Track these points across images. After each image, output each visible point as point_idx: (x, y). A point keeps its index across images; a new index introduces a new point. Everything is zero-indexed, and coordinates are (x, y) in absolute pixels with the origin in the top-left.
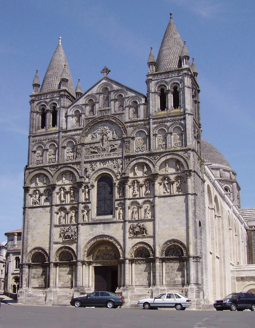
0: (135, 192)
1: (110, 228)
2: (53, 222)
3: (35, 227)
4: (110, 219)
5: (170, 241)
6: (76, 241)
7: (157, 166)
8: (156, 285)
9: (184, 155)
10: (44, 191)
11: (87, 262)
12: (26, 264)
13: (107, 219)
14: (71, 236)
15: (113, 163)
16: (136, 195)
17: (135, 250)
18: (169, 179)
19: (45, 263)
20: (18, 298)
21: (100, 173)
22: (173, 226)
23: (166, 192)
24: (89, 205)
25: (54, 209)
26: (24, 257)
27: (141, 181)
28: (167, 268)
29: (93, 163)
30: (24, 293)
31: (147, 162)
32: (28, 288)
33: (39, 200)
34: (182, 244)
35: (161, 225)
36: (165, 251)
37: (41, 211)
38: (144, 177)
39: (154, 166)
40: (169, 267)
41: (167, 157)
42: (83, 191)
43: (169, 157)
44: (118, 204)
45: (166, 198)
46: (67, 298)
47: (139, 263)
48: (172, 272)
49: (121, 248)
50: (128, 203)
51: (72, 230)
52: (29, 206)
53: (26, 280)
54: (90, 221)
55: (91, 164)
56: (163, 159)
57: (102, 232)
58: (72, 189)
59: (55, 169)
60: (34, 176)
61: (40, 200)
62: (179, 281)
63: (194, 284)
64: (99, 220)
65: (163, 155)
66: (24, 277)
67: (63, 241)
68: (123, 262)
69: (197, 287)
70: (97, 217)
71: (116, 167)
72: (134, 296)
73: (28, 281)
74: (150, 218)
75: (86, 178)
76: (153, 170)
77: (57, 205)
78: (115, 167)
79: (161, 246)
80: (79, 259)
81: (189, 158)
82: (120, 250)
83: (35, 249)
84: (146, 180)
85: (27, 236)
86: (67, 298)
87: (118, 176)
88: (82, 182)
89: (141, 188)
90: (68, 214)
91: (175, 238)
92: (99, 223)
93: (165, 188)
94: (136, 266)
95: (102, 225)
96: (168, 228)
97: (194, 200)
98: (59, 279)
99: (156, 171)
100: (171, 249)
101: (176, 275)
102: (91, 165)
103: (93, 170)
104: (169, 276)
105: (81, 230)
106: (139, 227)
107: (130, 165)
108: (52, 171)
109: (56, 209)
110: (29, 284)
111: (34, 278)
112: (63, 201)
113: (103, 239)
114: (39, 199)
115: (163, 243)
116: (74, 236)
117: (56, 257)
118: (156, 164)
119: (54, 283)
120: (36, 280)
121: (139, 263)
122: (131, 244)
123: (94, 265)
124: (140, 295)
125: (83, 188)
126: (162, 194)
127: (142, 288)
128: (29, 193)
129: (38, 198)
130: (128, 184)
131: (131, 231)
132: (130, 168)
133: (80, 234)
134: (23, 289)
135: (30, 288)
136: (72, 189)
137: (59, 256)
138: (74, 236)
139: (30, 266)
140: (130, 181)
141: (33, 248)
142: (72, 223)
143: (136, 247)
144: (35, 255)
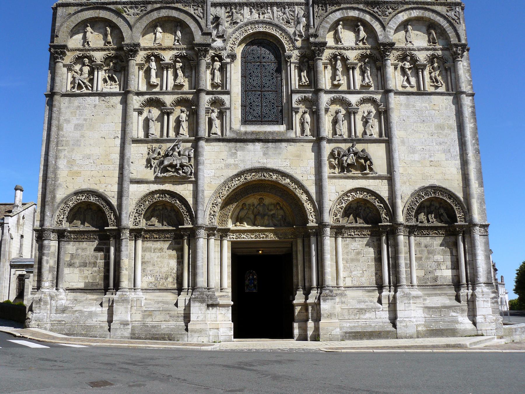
0: (337, 78)
1: (280, 154)
2: (128, 130)
3: (78, 141)
4: (278, 133)
5: (424, 189)
6: (194, 179)
7: (390, 28)
8: (400, 286)
9: (448, 14)
10: (106, 59)
11: (220, 230)
12: (54, 231)
13: (272, 133)
14: (178, 165)
15: (284, 13)
16: (339, 85)
17: (344, 205)
18: (414, 60)
19: (106, 228)
20: (30, 315)
21: (252, 32)
22: (431, 156)
23: (407, 85)
24: (225, 97)
25: (132, 101)
26: (48, 213)
27: (352, 56)
28: (418, 249)
29: (233, 7)
30: (46, 303)
31: (368, 18)
32: (56, 289)
33: (91, 81)
34: (451, 195)
35: (403, 155)
36: (414, 211)
37: (95, 106)
38: (359, 49)
39: (384, 27)
40: (420, 247)
41: (411, 14)
42: (208, 68)
43: (415, 13)
44: (300, 102)
45: (412, 98)
46: (168, 317)
47: (350, 235)
48: (428, 258)
49: (310, 198)
50: (325, 99)
51: (182, 153)
52: (64, 91)
53: (51, 269)
54: (229, 134)
55: (228, 10)
56: (403, 16)
57: (261, 161)
58: (178, 59)
59: (139, 12)
60: (80, 22)
61: (93, 79)
62: (445, 278)
63: (484, 283)
64: (252, 133)
65: (403, 8)
66: (47, 263)
67: (156, 177)
68: (319, 232)
69: (491, 291)
70: (244, 127)
71: (291, 21)
72: (346, 310)
73: (55, 273)
74: (376, 136)
75: (216, 39)
76: (381, 35)
77: (139, 94)
78: (288, 22)
79: (406, 199)
80: (200, 221)
81: (458, 21)
82: (308, 206)
83: (76, 193)
84: (362, 58)
85: (55, 163)
86: (168, 315)
87: (297, 40)
88: (209, 45)
89: (351, 71)
90: (168, 114)
91: (437, 184)
92: (253, 141)
93: (406, 77)
94: (344, 243)
95: (258, 146)
96: (419, 161)
97: (471, 107)
98: (143, 270)
99: (388, 38)
100: (424, 207)
101: (439, 264)
102: (228, 12)
103: (236, 23)
104: (420, 267)
105: (205, 153)
106: (356, 154)
107: (328, 20)
108: (128, 15)
109: (136, 102)
110: (59, 280)
111: (70, 265)
112: (155, 86)
113: (263, 178)
114: (92, 77)
115: (410, 193)
116: (187, 166)
117: (137, 215)
118: (388, 23)
119: (129, 280)
120: (77, 271)
121: (350, 235)
122: (334, 191)
123: (233, 237)
124: (361, 309)
125: (208, 59)
126: (400, 89)
127: (360, 293)
128: (64, 62)
129: (87, 75)
130: (322, 59)
131: (335, 162)
132: (328, 26)
133: (204, 163)
134: (43, 293)
135: (61, 290)
136: (178, 59)
137: (143, 212)
138: (187, 166)
139: (61, 235)
140: (327, 54)
141: (71, 190)
142: (182, 137)
143: (346, 198)
144: (75, 210)
